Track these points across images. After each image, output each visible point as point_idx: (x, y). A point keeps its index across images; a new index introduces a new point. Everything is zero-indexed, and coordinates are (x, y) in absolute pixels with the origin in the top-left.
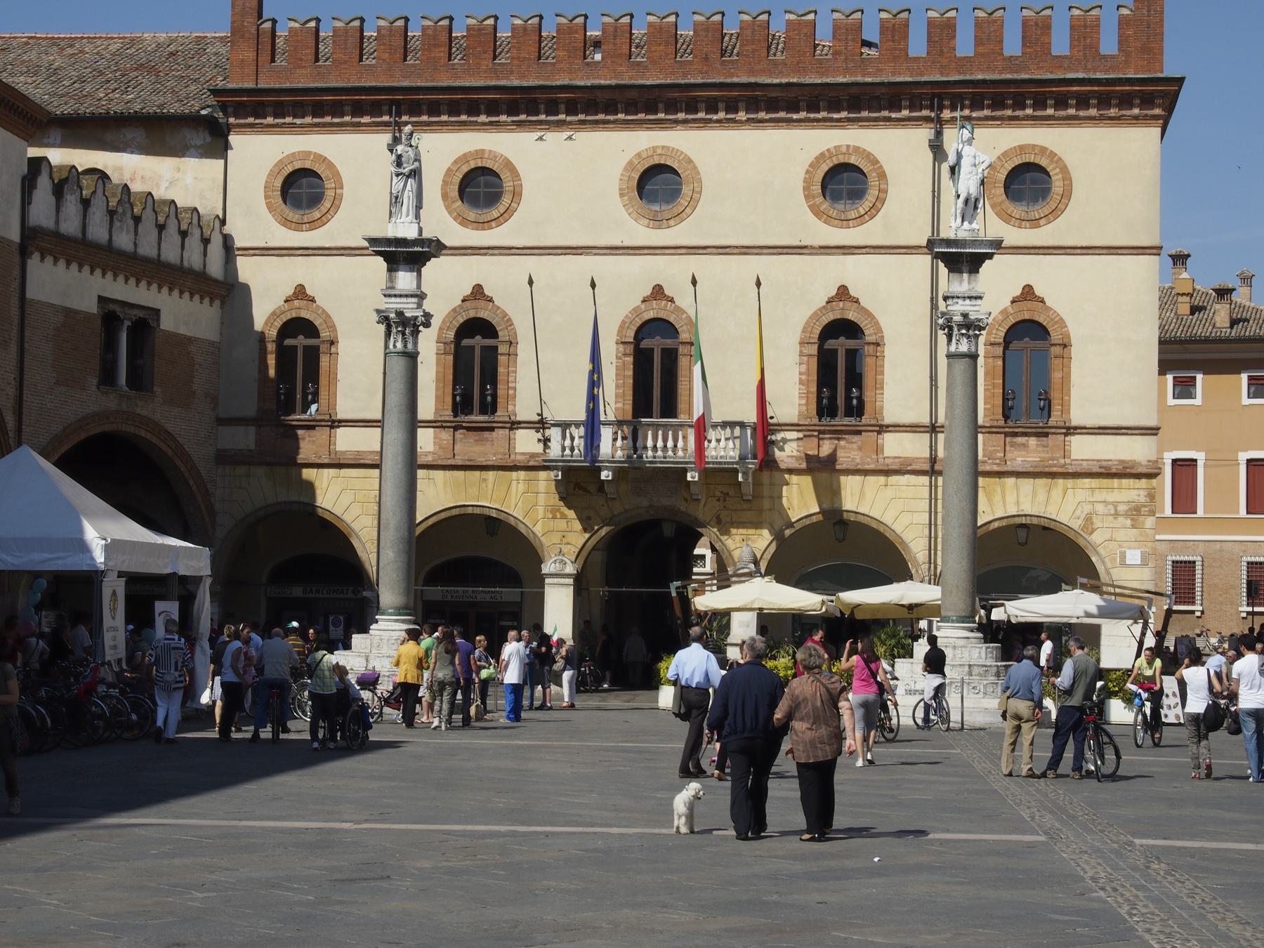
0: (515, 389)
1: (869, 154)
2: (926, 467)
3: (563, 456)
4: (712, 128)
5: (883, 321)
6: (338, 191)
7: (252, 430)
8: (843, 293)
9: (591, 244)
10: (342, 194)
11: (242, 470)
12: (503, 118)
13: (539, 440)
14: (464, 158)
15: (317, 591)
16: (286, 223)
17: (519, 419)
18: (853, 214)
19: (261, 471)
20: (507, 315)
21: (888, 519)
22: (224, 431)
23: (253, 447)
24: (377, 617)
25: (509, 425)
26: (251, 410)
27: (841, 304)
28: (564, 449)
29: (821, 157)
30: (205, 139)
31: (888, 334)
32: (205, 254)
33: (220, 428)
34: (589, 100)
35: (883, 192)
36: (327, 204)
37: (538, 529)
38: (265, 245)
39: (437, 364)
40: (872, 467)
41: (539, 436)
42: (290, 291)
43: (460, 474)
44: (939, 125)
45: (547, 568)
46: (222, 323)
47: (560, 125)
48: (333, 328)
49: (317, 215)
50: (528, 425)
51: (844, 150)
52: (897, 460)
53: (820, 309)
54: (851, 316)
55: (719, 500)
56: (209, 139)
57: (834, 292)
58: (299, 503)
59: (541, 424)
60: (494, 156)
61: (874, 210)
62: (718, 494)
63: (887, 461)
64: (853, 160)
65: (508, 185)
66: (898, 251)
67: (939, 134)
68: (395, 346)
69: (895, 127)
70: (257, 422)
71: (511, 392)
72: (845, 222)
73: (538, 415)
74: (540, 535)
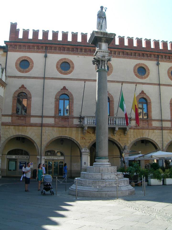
0: (73, 110)
1: (146, 65)
2: (161, 129)
3: (88, 124)
4: (114, 57)
5: (151, 98)
6: (33, 65)
7: (10, 118)
8: (143, 92)
9: (90, 79)
10: (33, 66)
11: (7, 127)
12: (70, 52)
13: (79, 121)
14: (62, 59)
15: (18, 157)
16: (20, 71)
17: (74, 116)
18: (144, 76)
19: (12, 127)
20: (71, 93)
21: (154, 139)
22: (3, 118)
23: (10, 122)
24: (96, 160)
25: (72, 118)
26: (10, 113)
27: (142, 94)
28: (88, 123)
29: (137, 65)
30: (2, 53)
31: (152, 101)
32: (2, 76)
33: (3, 117)
34: (89, 49)
35: (149, 73)
36: (30, 67)
37: (79, 142)
38: (15, 76)
39: (55, 104)
40: (151, 128)
41: (79, 120)
42: (20, 86)
43: (60, 129)
44: (158, 61)
45: (83, 150)
46: (4, 93)
47: (83, 55)
48: (31, 95)
49: (27, 69)
50: (77, 118)
51: (141, 64)
52: (155, 127)
53: (138, 95)
54: (145, 97)
55: (119, 135)
56: (3, 53)
57: (141, 92)
58: (22, 135)
59: (81, 118)
60: (68, 59)
61: (148, 76)
62: (119, 134)
63: (153, 127)
64: (143, 66)
65: (71, 66)
66: (153, 84)
67: (158, 62)
68: (101, 68)
69: (150, 60)
70: (11, 116)
71: (72, 110)
72: (142, 78)
73: (80, 115)
74: (79, 143)
